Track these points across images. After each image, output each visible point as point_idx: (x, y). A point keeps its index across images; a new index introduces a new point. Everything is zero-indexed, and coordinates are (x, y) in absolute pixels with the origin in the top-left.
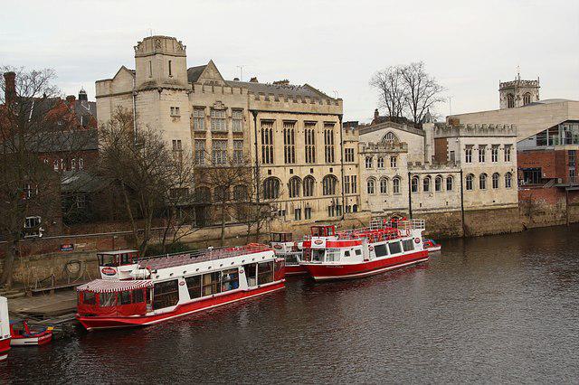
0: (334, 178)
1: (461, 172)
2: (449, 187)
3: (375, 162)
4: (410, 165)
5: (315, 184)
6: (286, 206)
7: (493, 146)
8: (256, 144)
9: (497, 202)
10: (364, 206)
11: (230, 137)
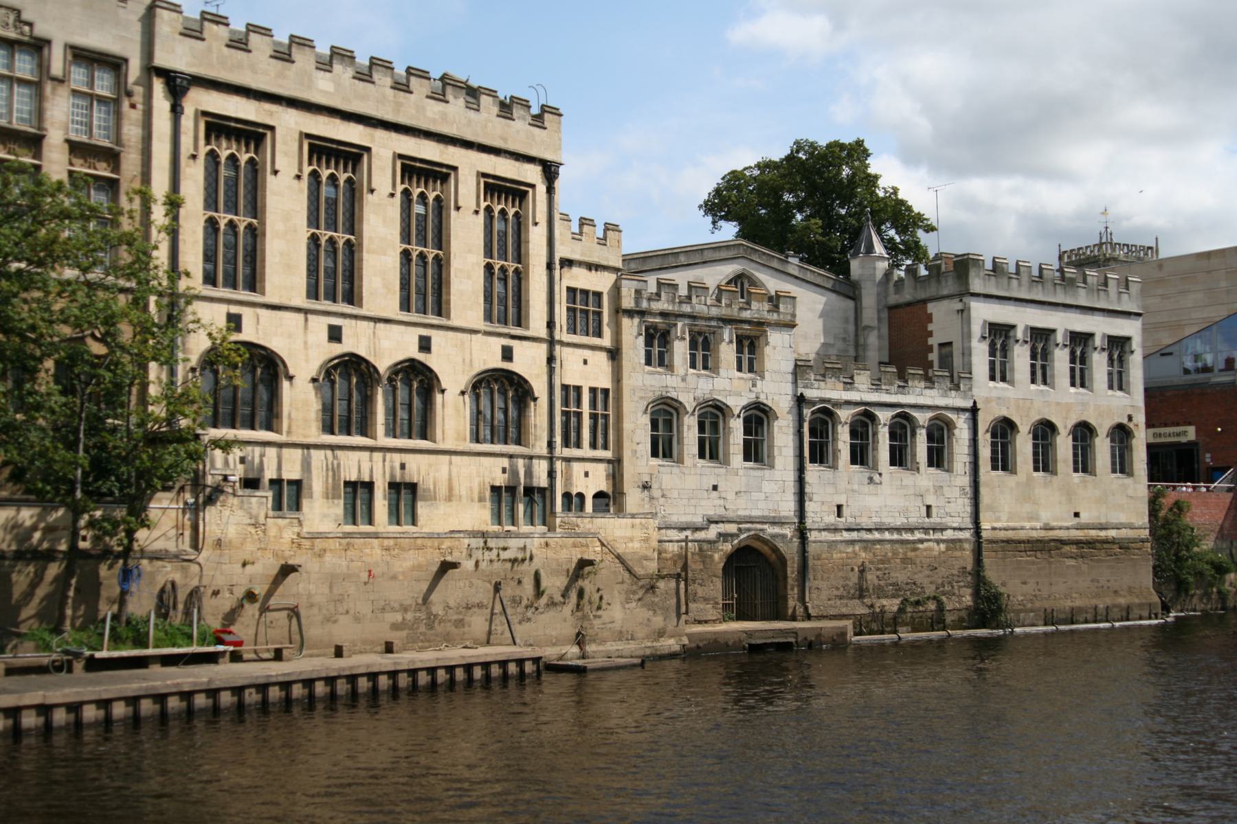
1: (974, 411)
2: (937, 458)
3: (680, 350)
4: (800, 369)
5: (438, 397)
6: (306, 465)
9: (1085, 518)
10: (633, 499)
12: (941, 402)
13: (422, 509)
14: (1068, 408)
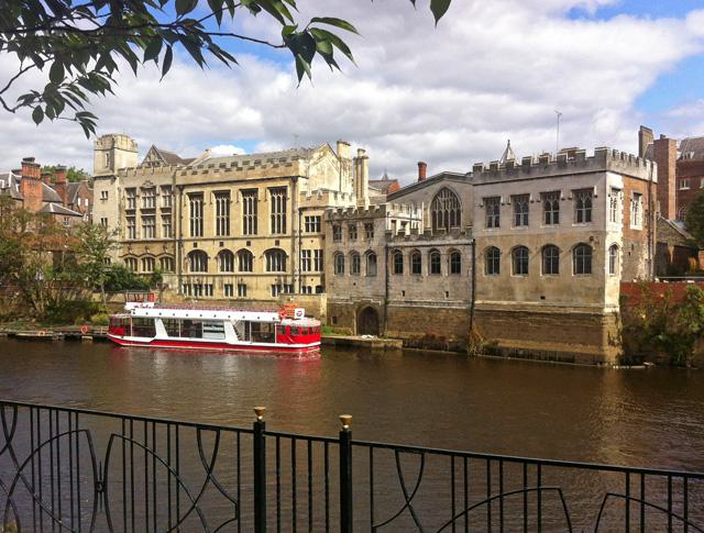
0: (285, 256)
1: (473, 244)
3: (344, 232)
6: (214, 281)
7: (545, 195)
8: (181, 217)
11: (159, 213)
12: (453, 242)
13: (248, 292)
14: (538, 236)
